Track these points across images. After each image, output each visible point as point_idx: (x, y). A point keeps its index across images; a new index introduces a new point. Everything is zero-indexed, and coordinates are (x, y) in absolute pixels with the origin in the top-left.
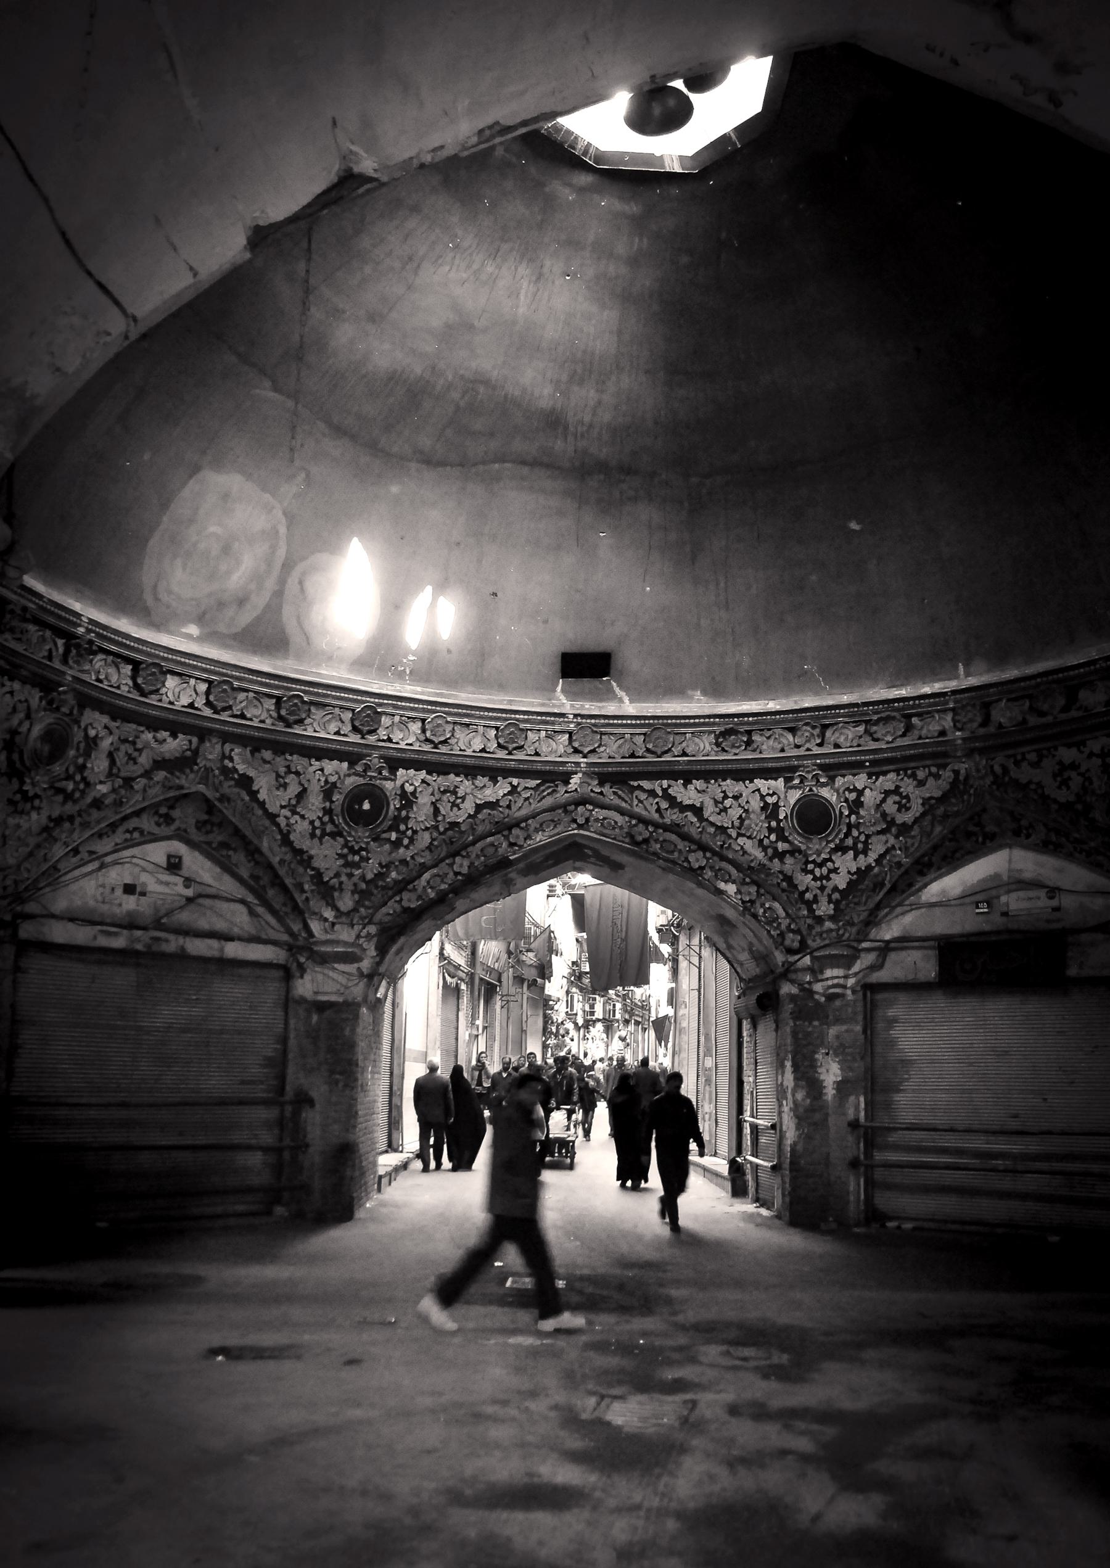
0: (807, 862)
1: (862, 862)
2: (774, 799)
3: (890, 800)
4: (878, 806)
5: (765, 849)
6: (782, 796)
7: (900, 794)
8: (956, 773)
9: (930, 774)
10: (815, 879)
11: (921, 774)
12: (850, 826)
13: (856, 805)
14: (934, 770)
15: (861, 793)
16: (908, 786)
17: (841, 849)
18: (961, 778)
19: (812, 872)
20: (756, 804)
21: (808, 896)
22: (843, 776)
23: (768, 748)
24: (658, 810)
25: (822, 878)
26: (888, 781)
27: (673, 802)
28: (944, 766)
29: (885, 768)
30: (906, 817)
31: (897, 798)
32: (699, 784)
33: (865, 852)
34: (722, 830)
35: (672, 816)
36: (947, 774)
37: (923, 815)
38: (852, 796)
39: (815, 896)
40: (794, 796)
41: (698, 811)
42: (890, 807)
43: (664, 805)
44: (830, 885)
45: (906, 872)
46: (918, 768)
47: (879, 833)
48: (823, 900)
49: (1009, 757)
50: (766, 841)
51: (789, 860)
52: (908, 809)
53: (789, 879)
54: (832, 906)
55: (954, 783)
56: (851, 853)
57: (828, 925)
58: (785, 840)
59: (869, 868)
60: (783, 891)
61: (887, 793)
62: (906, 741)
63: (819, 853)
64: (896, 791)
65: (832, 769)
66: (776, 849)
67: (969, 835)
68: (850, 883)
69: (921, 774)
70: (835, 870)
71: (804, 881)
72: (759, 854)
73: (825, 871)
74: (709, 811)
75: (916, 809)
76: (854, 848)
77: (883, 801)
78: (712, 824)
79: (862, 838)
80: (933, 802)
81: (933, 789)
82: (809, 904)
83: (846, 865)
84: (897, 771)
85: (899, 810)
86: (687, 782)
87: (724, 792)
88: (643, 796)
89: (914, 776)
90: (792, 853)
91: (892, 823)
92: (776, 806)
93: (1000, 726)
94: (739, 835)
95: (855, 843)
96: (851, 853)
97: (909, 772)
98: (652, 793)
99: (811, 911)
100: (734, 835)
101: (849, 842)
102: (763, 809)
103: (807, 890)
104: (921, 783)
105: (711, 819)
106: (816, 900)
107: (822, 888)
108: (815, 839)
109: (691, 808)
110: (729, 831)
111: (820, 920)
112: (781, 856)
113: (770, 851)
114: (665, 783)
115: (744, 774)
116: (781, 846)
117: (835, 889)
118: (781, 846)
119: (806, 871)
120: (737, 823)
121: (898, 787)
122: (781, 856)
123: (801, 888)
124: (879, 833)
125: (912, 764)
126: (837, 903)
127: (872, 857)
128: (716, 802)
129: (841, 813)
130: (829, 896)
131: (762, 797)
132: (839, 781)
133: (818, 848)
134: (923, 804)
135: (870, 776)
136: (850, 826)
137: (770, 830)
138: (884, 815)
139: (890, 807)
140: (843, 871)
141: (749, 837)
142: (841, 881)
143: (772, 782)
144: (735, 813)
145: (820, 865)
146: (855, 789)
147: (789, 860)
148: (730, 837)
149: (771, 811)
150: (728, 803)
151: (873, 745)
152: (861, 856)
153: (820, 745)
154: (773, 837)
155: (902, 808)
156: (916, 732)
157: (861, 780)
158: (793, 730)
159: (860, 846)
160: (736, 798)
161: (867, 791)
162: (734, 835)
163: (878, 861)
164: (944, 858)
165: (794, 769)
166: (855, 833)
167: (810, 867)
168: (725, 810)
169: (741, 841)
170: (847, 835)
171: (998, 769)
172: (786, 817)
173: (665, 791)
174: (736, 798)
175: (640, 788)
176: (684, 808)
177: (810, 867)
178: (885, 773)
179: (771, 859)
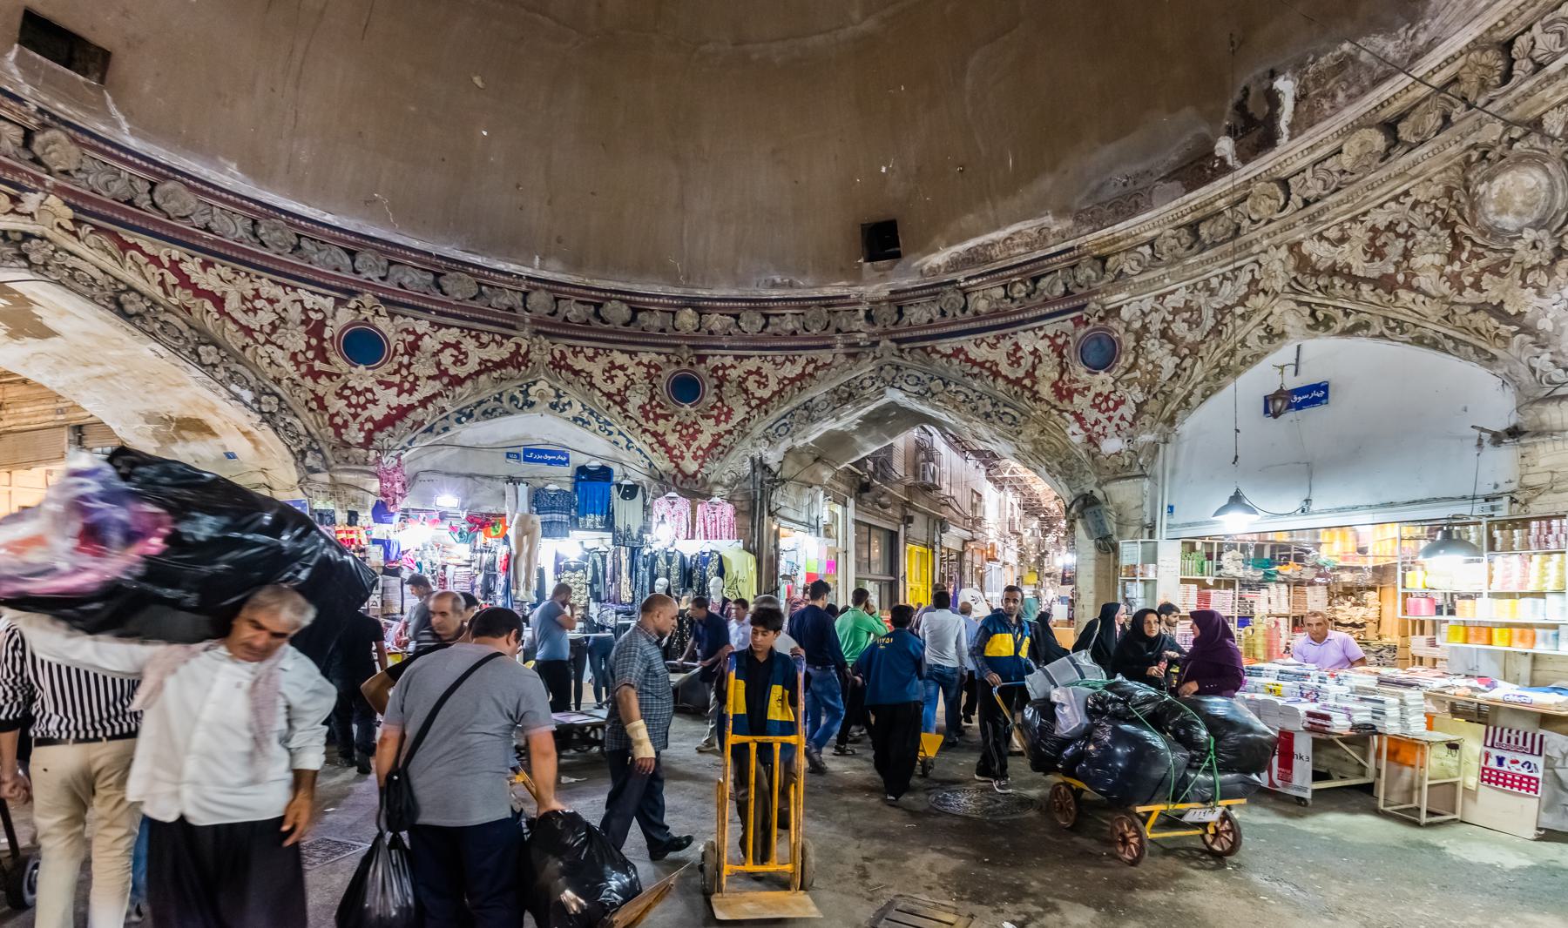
1: (405, 400)
2: (319, 316)
3: (449, 351)
4: (435, 354)
5: (298, 364)
6: (329, 314)
7: (459, 349)
8: (519, 346)
10: (350, 405)
11: (485, 338)
12: (401, 364)
13: (412, 349)
14: (498, 338)
15: (420, 337)
16: (469, 344)
17: (388, 385)
18: (523, 351)
19: (347, 398)
20: (295, 314)
21: (338, 420)
22: (405, 316)
25: (357, 405)
27: (185, 281)
28: (508, 337)
30: (461, 372)
31: (456, 353)
33: (410, 392)
34: (248, 331)
36: (510, 346)
37: (478, 373)
38: (411, 338)
39: (346, 422)
40: (345, 316)
42: (447, 358)
43: (171, 279)
44: (366, 414)
45: (447, 418)
46: (483, 331)
47: (429, 378)
48: (354, 426)
49: (569, 346)
50: (300, 358)
51: (323, 380)
52: (463, 364)
53: (319, 400)
54: (363, 434)
56: (395, 390)
58: (327, 361)
59: (411, 407)
60: (311, 410)
61: (446, 345)
62: (476, 304)
64: (457, 346)
66: (311, 368)
67: (513, 398)
69: (485, 338)
70: (374, 402)
72: (289, 367)
73: (362, 400)
74: (232, 304)
75: (472, 365)
76: (401, 386)
77: (441, 351)
78: (235, 321)
79: (411, 378)
80: (489, 364)
81: (495, 353)
84: (462, 329)
85: (454, 363)
87: (256, 290)
88: (142, 260)
89: (477, 338)
90: (329, 375)
91: (444, 373)
92: (321, 324)
93: (566, 319)
94: (268, 342)
95: (402, 383)
96: (395, 390)
97: (473, 333)
98: (155, 260)
100: (262, 339)
101: (397, 379)
102: (303, 322)
103: (337, 414)
105: (234, 315)
106: (346, 424)
109: (210, 295)
110: (256, 335)
111: (347, 445)
113: (304, 368)
114: (176, 253)
116: (318, 365)
117: (370, 419)
118: (318, 365)
119: (340, 395)
120: (267, 329)
121: (459, 343)
122: (316, 375)
123: (332, 411)
124: (429, 378)
128: (244, 299)
129: (396, 350)
130: (362, 424)
131: (305, 310)
132: (399, 320)
133: (361, 376)
134: (480, 364)
135: (432, 324)
136: (401, 364)
138: (438, 364)
139: (447, 358)
141: (281, 347)
142: (378, 412)
143: (320, 299)
145: (358, 394)
146: (414, 332)
147: (323, 380)
148: (256, 341)
149: (316, 330)
150: (258, 303)
152: (405, 395)
154: (310, 354)
159: (407, 386)
160: (271, 301)
161: (427, 337)
162: (262, 339)
163: (424, 403)
164: (485, 413)
165: (353, 293)
166: (404, 372)
167: (347, 392)
168: (255, 310)
169: (269, 348)
170: (396, 372)
171: (557, 355)
172: (332, 338)
176: (199, 293)
177: (347, 392)
178: (448, 327)
179: (303, 376)
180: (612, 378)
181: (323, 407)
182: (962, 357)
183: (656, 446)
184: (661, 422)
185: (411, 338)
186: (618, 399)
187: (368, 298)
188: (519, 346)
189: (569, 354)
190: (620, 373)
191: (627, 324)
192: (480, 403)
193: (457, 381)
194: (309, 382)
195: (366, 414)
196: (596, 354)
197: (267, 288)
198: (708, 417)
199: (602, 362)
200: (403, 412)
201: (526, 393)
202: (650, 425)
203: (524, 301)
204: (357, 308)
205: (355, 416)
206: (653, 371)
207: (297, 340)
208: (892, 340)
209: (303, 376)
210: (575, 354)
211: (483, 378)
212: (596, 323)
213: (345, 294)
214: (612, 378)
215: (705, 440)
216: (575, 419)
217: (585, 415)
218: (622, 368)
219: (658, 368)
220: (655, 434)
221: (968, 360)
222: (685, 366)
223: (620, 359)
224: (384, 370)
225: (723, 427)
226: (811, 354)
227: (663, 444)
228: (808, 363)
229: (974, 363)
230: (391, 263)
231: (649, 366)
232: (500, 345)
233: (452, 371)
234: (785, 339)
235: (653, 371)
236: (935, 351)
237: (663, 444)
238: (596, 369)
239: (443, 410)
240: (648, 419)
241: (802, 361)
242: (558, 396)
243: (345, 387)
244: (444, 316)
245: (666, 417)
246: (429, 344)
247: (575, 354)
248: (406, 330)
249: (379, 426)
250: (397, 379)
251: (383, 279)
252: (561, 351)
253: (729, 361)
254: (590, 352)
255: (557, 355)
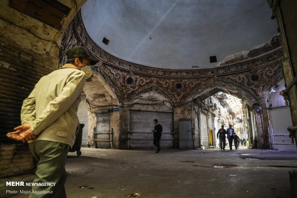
0: (126, 88)
8: (152, 79)
9: (148, 79)
10: (126, 91)
11: (147, 78)
13: (136, 81)
14: (149, 78)
15: (137, 79)
16: (144, 80)
17: (131, 87)
20: (122, 76)
23: (126, 67)
24: (108, 72)
26: (142, 78)
28: (150, 78)
29: (142, 76)
30: (142, 84)
32: (115, 70)
33: (135, 88)
34: (116, 79)
35: (110, 74)
36: (150, 79)
37: (145, 85)
40: (128, 76)
41: (113, 75)
42: (141, 82)
43: (109, 72)
44: (128, 92)
50: (121, 83)
51: (123, 87)
53: (122, 90)
55: (151, 81)
57: (126, 99)
58: (124, 83)
59: (134, 91)
61: (141, 80)
63: (128, 87)
64: (142, 80)
65: (135, 74)
68: (131, 93)
71: (125, 91)
75: (144, 83)
81: (148, 81)
82: (124, 95)
83: (132, 89)
86: (113, 69)
88: (107, 69)
89: (146, 78)
90: (124, 86)
91: (140, 85)
94: (118, 81)
98: (108, 69)
99: (124, 96)
102: (123, 77)
104: (146, 80)
107: (126, 93)
108: (129, 84)
111: (125, 98)
112: (122, 86)
113: (121, 85)
114: (110, 68)
115: (123, 70)
117: (128, 93)
125: (146, 76)
126: (128, 96)
127: (136, 89)
131: (123, 75)
133: (129, 86)
137: (123, 81)
138: (139, 83)
140: (130, 91)
142: (129, 92)
144: (119, 77)
145: (127, 89)
147: (123, 87)
149: (124, 78)
151: (141, 72)
153: (134, 69)
154: (123, 82)
155: (142, 83)
156: (147, 72)
157: (138, 77)
158: (130, 66)
163: (136, 90)
166: (134, 85)
167: (126, 89)
169: (118, 82)
173: (110, 69)
174: (119, 74)
175: (107, 67)
178: (142, 77)
180: (166, 85)
181: (123, 92)
182: (230, 79)
183: (173, 97)
184: (174, 92)
185: (136, 79)
186: (167, 88)
187: (132, 73)
188: (152, 79)
189: (159, 81)
190: (167, 84)
191: (169, 75)
192: (144, 90)
193: (142, 86)
194: (121, 87)
195: (128, 92)
196: (164, 80)
197: (119, 72)
198: (183, 91)
199: (165, 82)
200: (133, 92)
201: (152, 88)
202: (172, 93)
203: (153, 72)
204: (130, 75)
205: (126, 93)
206: (173, 83)
207: (121, 80)
208: (217, 76)
209: (121, 86)
210: (160, 80)
211: (146, 85)
212: (164, 75)
213: (128, 72)
214: (166, 85)
215: (182, 96)
216: (159, 93)
217: (161, 92)
218: (168, 83)
219: (174, 82)
220: (173, 95)
221: (231, 79)
222: (179, 82)
223: (168, 81)
224: (132, 85)
225: (185, 93)
226: (201, 79)
227: (174, 97)
228: (201, 81)
229: (232, 80)
230: (135, 67)
231: (172, 82)
232: (149, 79)
233: (141, 85)
234: (197, 76)
235: (173, 83)
236: (224, 78)
237: (174, 97)
238: (163, 83)
239: (139, 91)
240: (172, 92)
241: (200, 80)
242: (157, 88)
243: (126, 88)
244: (141, 75)
245: (175, 91)
246: (138, 80)
247: (160, 80)
248: (136, 78)
249: (129, 94)
250: (133, 86)
251: (134, 69)
252: (158, 80)
253: (187, 81)
254: (163, 80)
255: (157, 81)
